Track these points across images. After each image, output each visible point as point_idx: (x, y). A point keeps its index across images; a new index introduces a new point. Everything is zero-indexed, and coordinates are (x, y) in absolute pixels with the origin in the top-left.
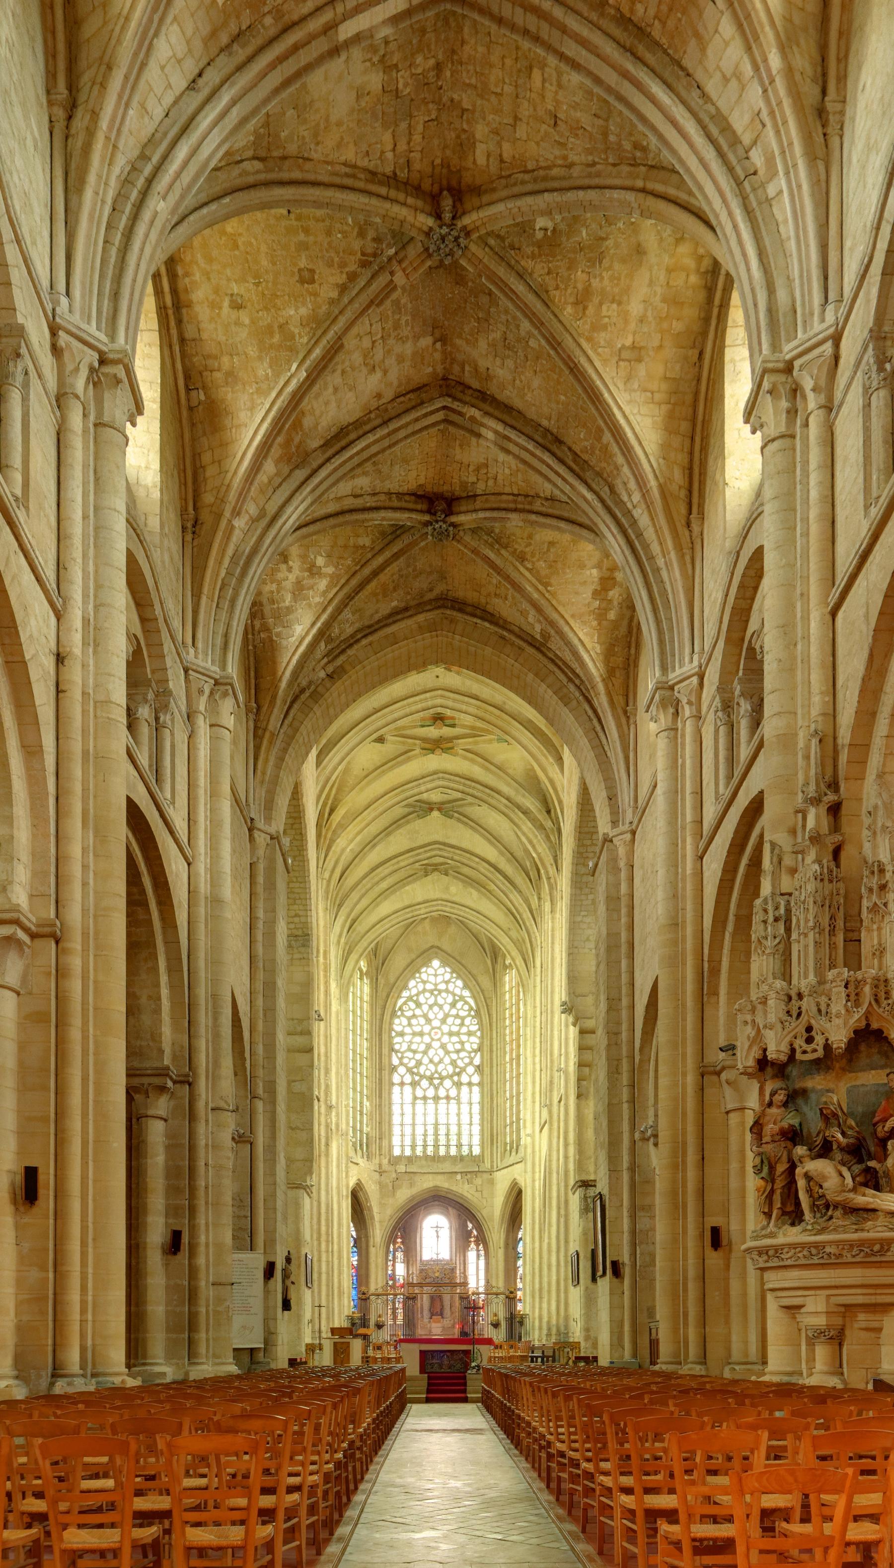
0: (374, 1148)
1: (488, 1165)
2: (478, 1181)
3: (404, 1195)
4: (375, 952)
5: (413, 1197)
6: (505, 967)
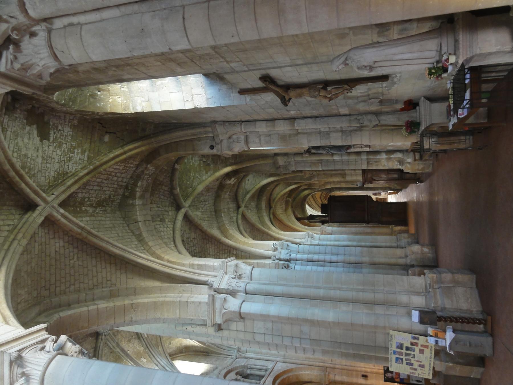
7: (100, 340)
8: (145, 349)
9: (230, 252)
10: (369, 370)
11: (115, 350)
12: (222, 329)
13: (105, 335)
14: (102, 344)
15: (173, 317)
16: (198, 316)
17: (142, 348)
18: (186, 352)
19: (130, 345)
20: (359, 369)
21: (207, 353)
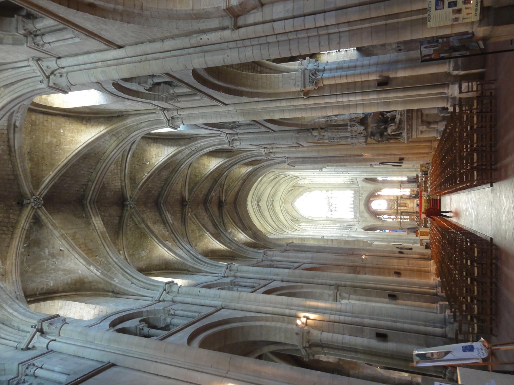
0: (351, 223)
1: (357, 189)
2: (362, 192)
3: (366, 215)
4: (293, 221)
5: (367, 212)
6: (297, 183)
7: (125, 211)
8: (170, 234)
9: (254, 69)
10: (402, 267)
11: (140, 226)
12: (239, 27)
13: (131, 207)
14: (127, 214)
15: (186, 9)
16: (213, 4)
17: (167, 233)
18: (211, 256)
19: (156, 226)
20: (391, 267)
21: (233, 257)
